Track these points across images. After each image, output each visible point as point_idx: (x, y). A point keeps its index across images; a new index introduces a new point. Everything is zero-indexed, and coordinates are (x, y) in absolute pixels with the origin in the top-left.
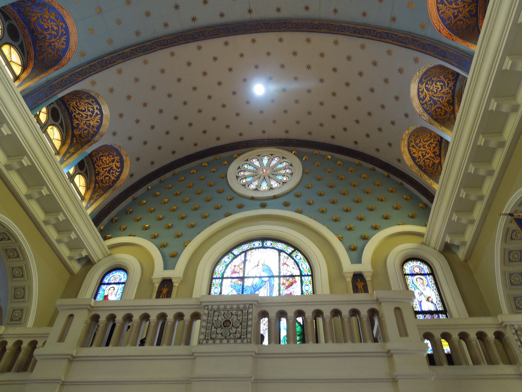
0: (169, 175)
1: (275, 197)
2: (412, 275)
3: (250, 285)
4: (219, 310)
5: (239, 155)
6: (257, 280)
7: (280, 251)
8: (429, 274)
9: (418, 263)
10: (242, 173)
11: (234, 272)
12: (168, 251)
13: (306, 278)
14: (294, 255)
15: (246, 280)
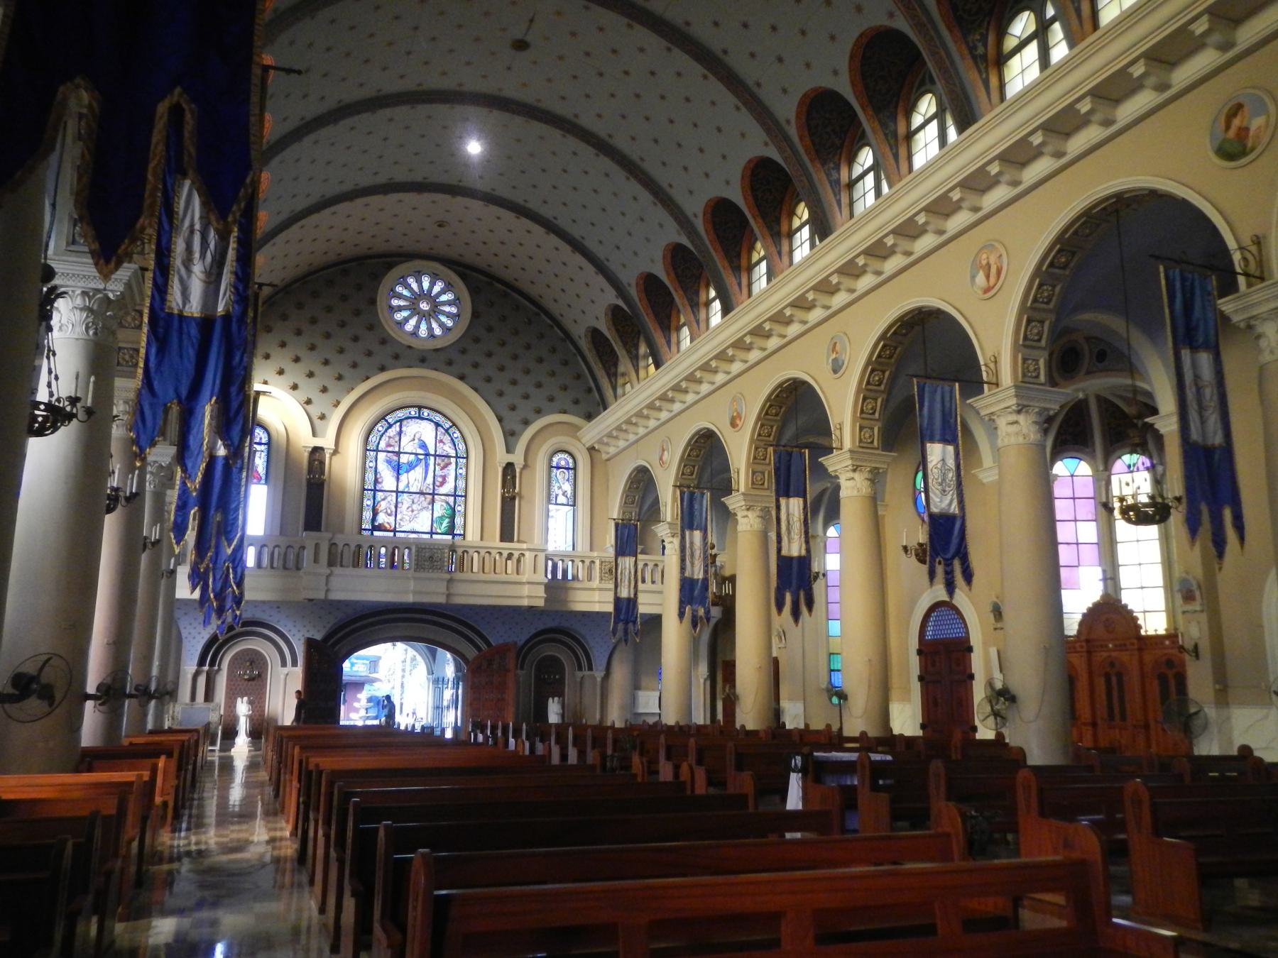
0: (298, 284)
1: (436, 350)
2: (558, 468)
3: (406, 462)
4: (425, 548)
5: (390, 267)
6: (412, 457)
7: (437, 425)
8: (571, 469)
9: (566, 456)
10: (396, 301)
11: (389, 445)
12: (315, 410)
13: (461, 460)
14: (450, 431)
15: (401, 455)
